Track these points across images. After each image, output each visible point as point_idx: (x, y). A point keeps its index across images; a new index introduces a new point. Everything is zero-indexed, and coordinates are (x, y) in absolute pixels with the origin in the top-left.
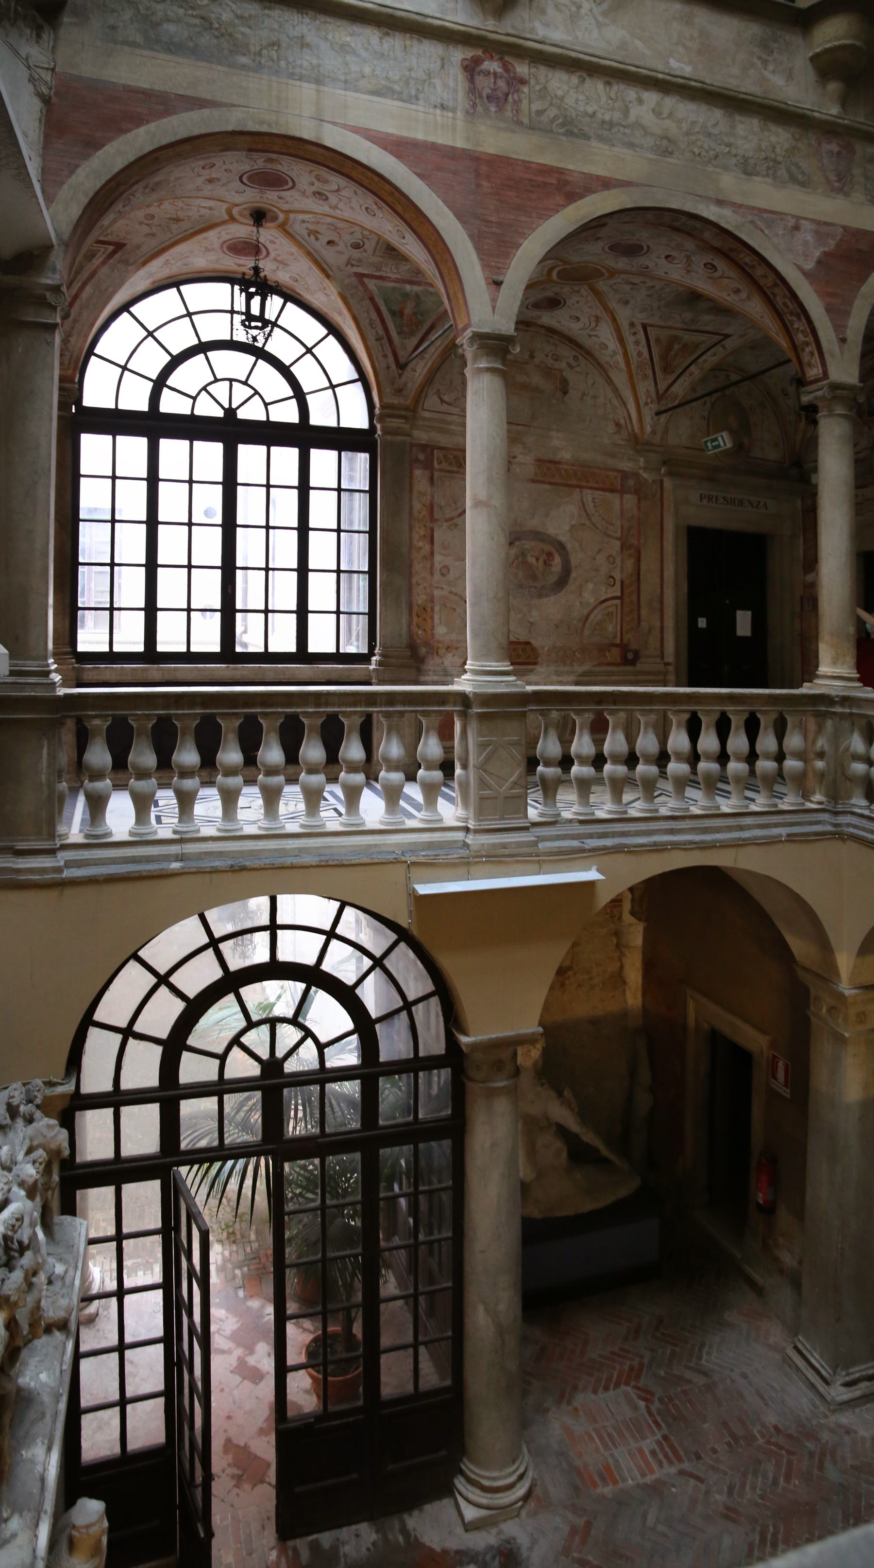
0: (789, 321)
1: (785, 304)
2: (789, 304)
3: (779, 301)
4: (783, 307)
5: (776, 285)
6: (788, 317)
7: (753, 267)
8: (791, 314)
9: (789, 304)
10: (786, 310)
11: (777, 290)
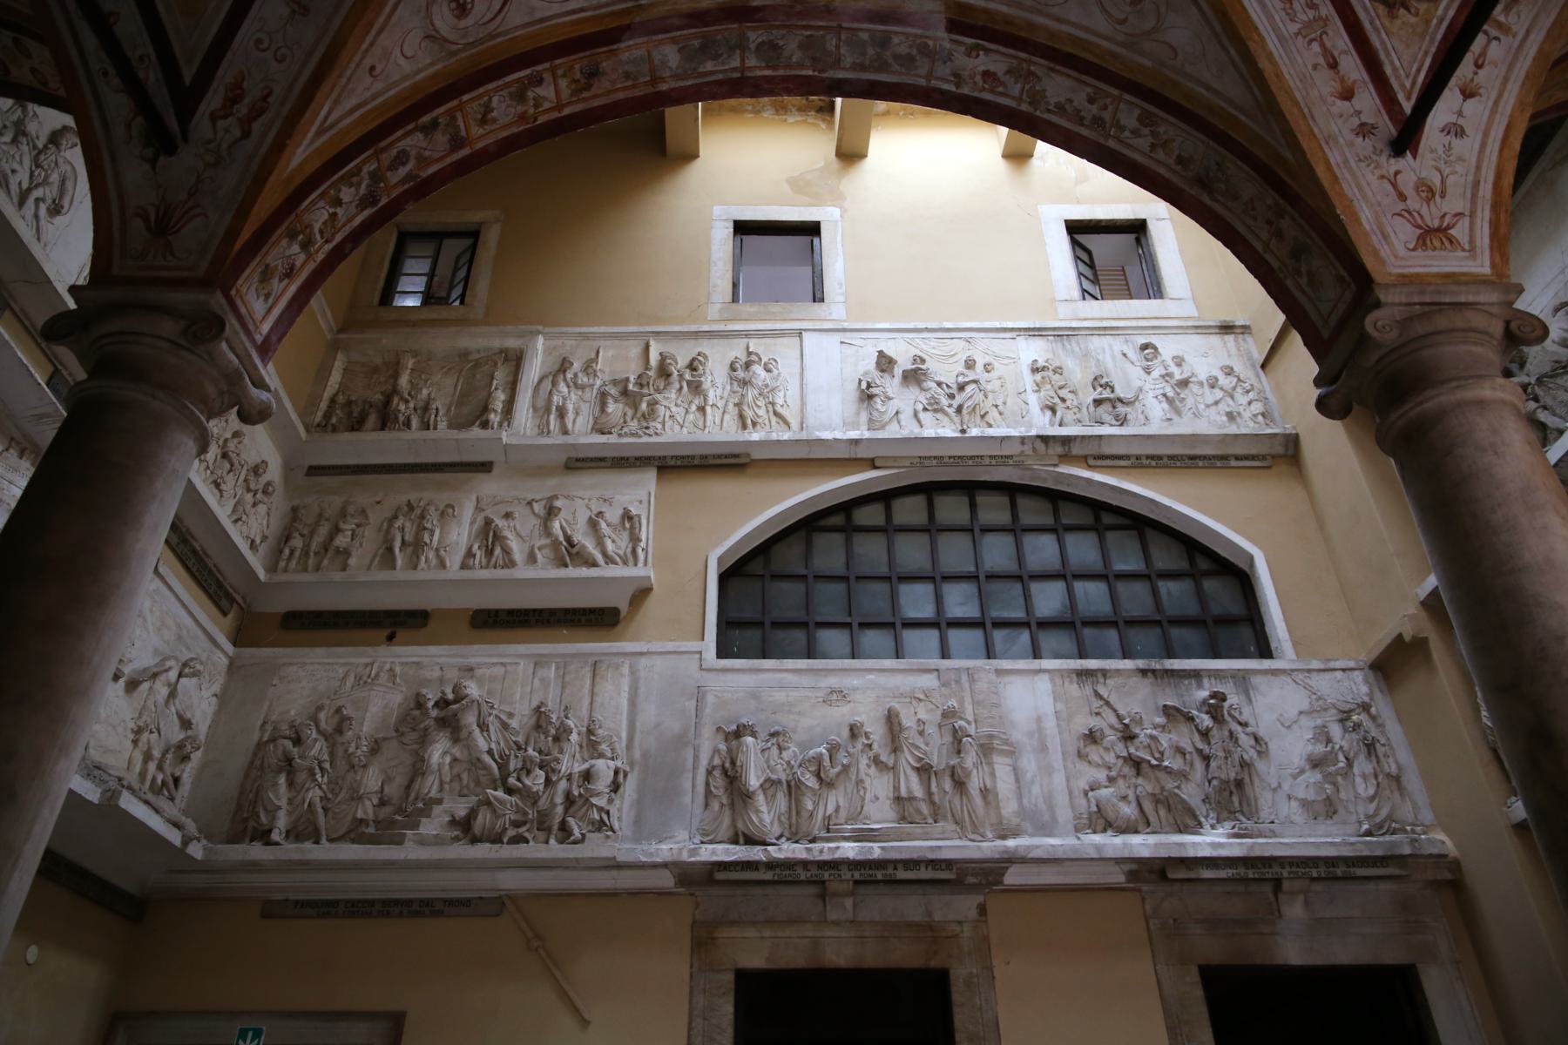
0: (359, 168)
1: (401, 158)
2: (403, 171)
3: (413, 142)
4: (394, 152)
5: (457, 142)
6: (366, 165)
7: (520, 97)
8: (375, 177)
9: (403, 171)
10: (386, 159)
11: (441, 139)
